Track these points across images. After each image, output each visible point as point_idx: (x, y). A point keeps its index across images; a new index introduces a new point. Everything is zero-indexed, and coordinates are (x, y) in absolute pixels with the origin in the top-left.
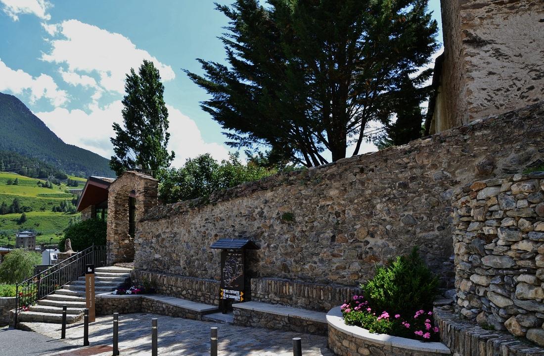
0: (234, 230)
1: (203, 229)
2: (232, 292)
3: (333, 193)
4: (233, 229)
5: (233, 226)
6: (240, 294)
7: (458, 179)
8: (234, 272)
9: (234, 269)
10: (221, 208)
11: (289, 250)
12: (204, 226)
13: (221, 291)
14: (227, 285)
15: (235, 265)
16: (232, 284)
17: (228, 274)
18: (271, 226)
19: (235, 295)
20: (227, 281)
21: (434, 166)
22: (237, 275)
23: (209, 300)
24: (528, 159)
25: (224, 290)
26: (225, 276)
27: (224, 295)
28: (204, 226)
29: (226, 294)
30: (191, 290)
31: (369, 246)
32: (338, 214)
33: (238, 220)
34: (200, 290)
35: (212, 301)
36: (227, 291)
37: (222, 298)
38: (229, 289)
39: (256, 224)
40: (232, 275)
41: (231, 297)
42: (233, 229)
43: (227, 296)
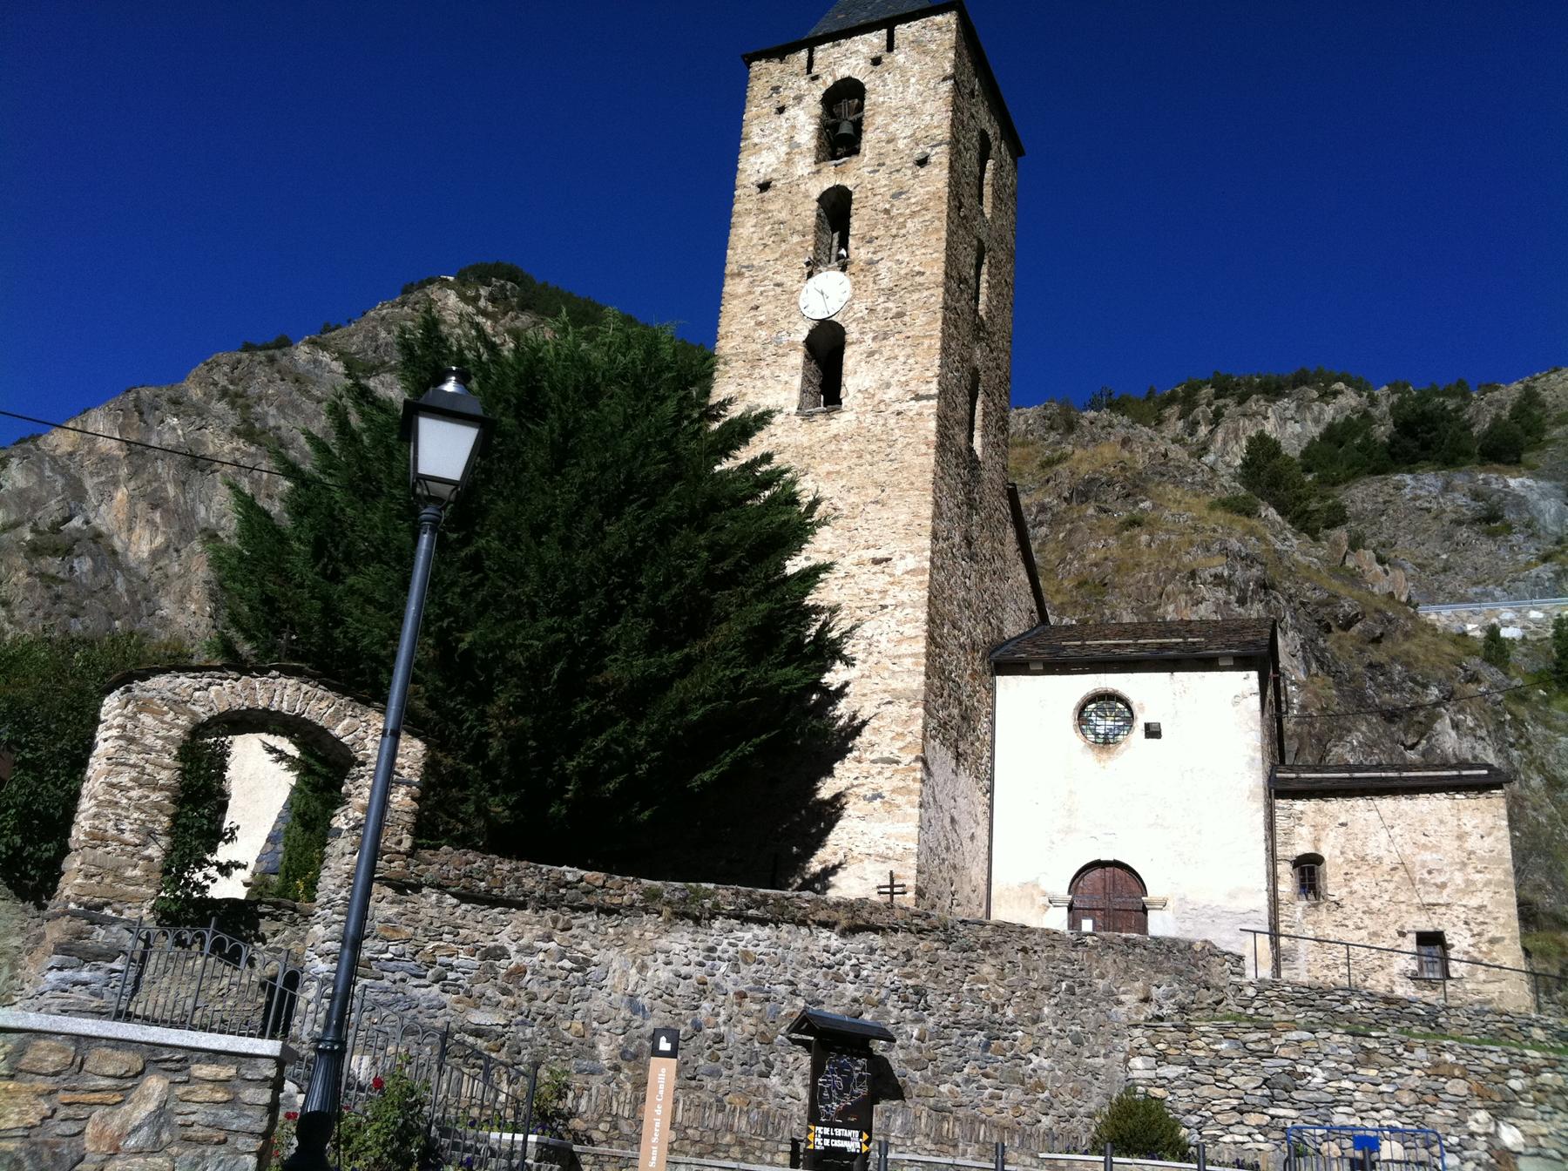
0: (793, 993)
1: (698, 973)
2: (839, 1132)
3: (985, 969)
4: (790, 988)
5: (791, 983)
6: (860, 1136)
7: (1123, 998)
8: (847, 1089)
9: (847, 1082)
10: (784, 935)
11: (916, 1055)
12: (701, 964)
13: (809, 1131)
14: (827, 1116)
15: (850, 1074)
16: (840, 1114)
17: (830, 1093)
18: (882, 1002)
19: (848, 1139)
20: (827, 1108)
21: (1102, 976)
22: (853, 1094)
23: (758, 1153)
24: (1173, 996)
25: (819, 1129)
26: (821, 1096)
27: (818, 1140)
28: (701, 964)
29: (823, 1136)
30: (696, 1128)
31: (1031, 1066)
32: (995, 1008)
33: (805, 973)
34: (730, 1129)
35: (768, 1158)
36: (827, 1131)
37: (811, 1147)
38: (832, 1125)
39: (850, 990)
40: (841, 1094)
41: (838, 1144)
42: (790, 988)
43: (827, 1142)
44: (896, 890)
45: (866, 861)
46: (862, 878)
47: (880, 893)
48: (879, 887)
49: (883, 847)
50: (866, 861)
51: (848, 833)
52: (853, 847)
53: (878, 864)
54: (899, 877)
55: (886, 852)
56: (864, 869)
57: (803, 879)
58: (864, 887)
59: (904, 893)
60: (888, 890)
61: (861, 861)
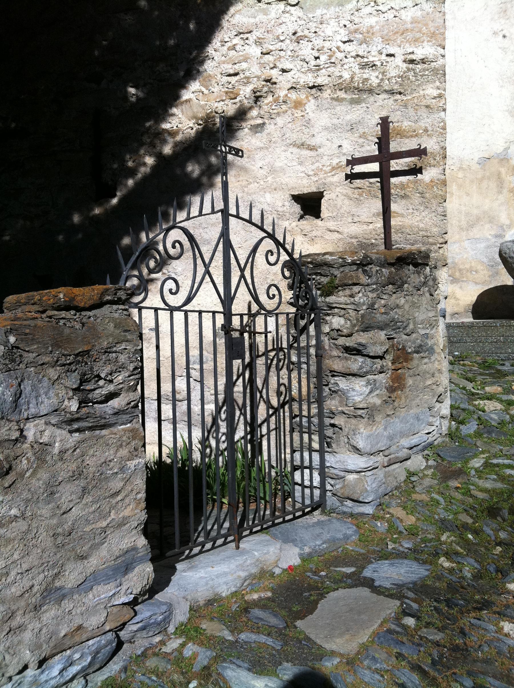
44: (395, 165)
45: (311, 105)
46: (302, 146)
47: (351, 177)
48: (353, 162)
49: (353, 65)
50: (311, 105)
51: (259, 42)
52: (275, 73)
53: (340, 109)
54: (401, 134)
55: (360, 75)
56: (308, 123)
57: (160, 157)
58: (310, 169)
59: (415, 171)
60: (375, 167)
61: (298, 105)
